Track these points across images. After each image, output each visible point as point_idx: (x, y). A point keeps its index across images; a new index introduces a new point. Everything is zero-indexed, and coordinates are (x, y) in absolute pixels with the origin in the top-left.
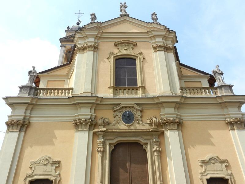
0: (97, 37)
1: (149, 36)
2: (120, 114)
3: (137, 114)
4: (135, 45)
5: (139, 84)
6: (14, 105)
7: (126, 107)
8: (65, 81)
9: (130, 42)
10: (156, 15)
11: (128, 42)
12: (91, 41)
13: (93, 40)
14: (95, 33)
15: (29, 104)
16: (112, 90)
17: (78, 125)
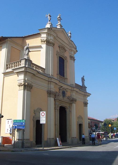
0: (55, 38)
1: (70, 48)
2: (61, 91)
3: (66, 93)
4: (65, 51)
5: (65, 77)
6: (27, 73)
7: (63, 88)
8: (20, 51)
9: (64, 49)
10: (71, 34)
11: (62, 48)
12: (51, 38)
13: (53, 39)
14: (55, 35)
15: (34, 74)
16: (59, 76)
17: (50, 93)
